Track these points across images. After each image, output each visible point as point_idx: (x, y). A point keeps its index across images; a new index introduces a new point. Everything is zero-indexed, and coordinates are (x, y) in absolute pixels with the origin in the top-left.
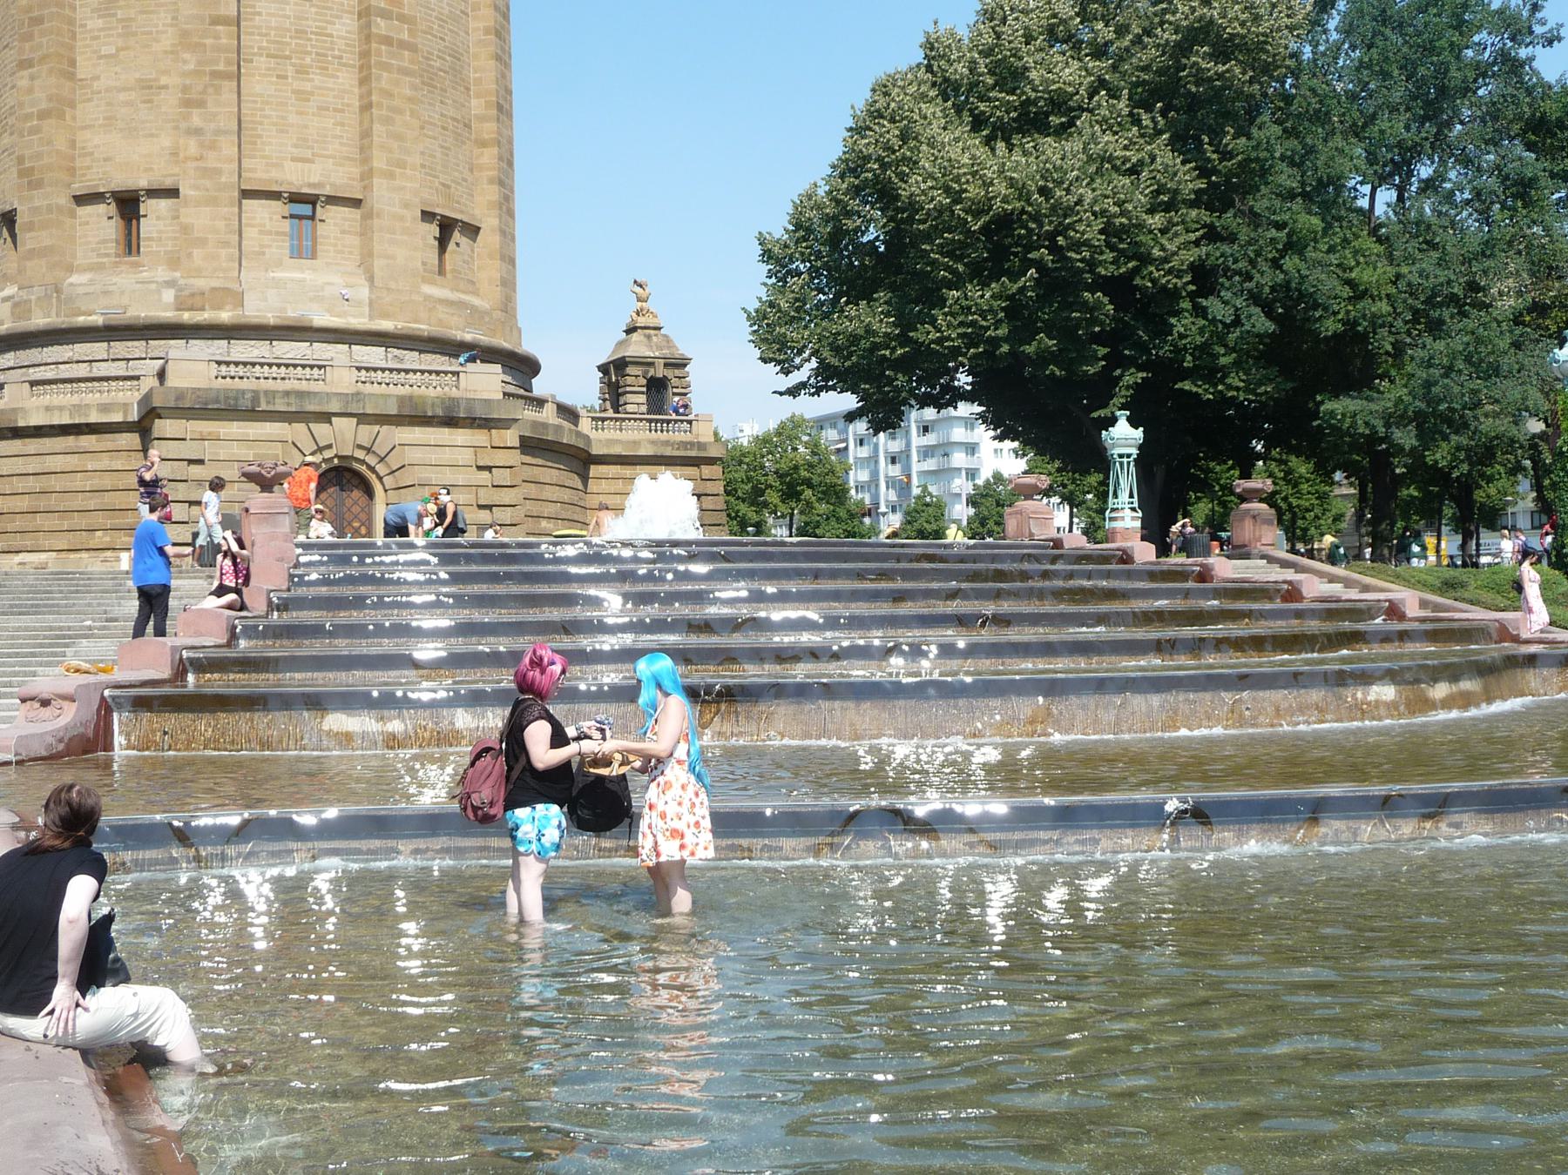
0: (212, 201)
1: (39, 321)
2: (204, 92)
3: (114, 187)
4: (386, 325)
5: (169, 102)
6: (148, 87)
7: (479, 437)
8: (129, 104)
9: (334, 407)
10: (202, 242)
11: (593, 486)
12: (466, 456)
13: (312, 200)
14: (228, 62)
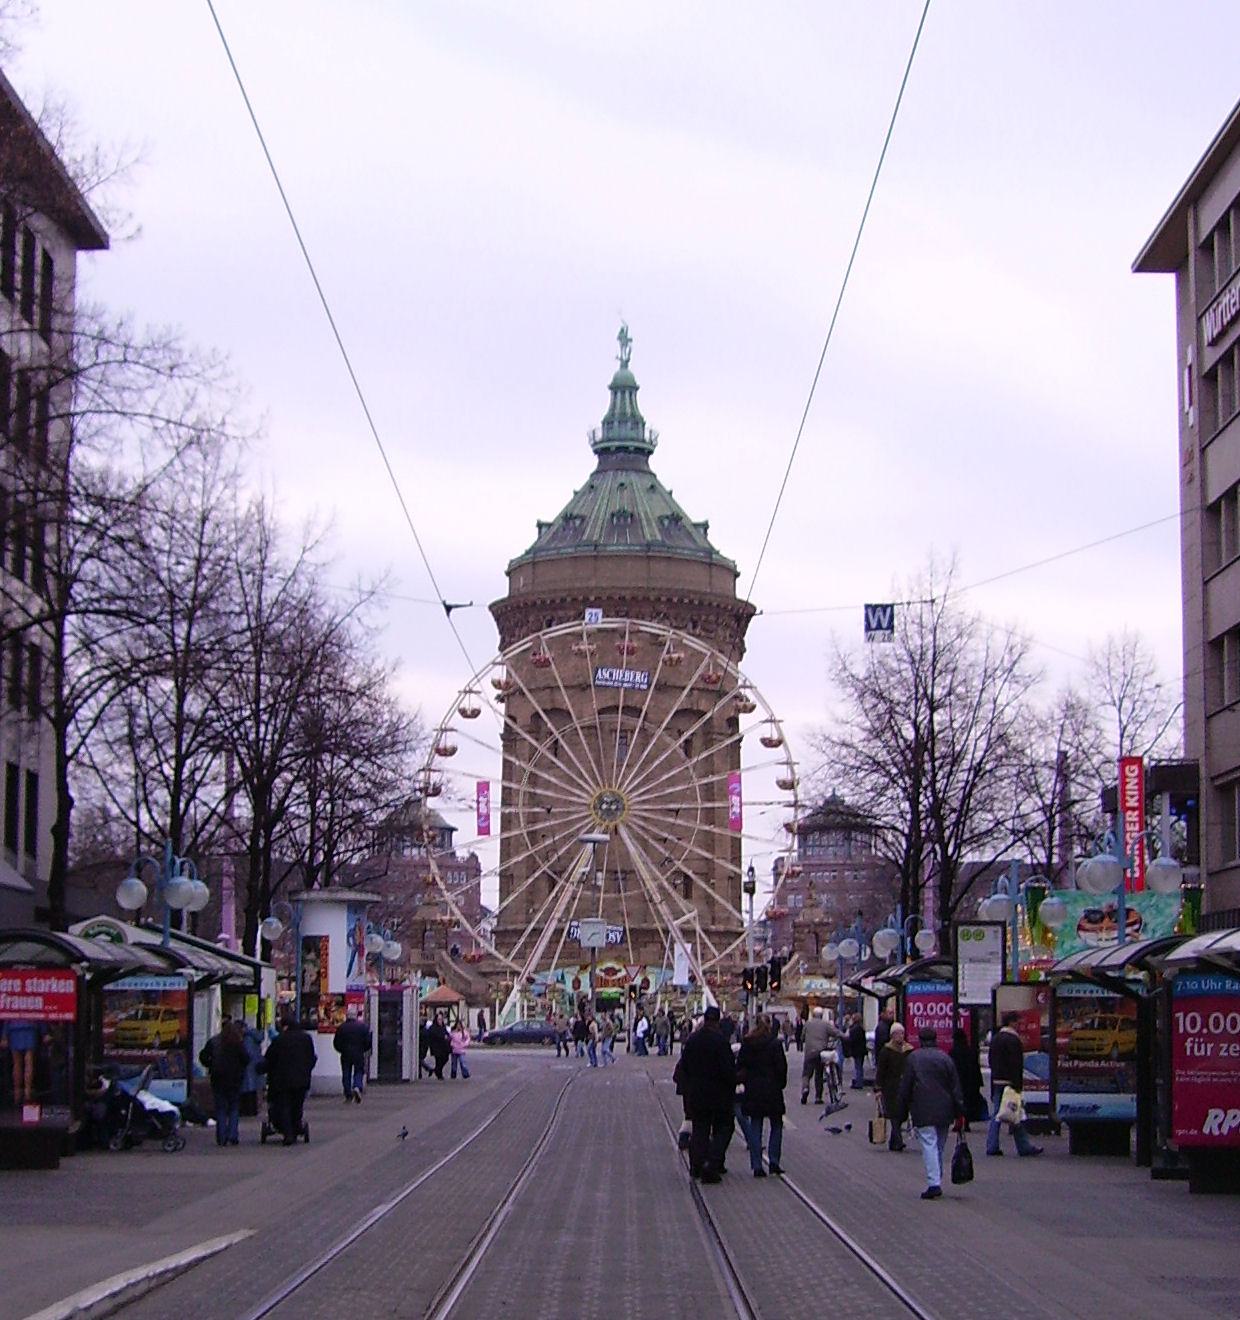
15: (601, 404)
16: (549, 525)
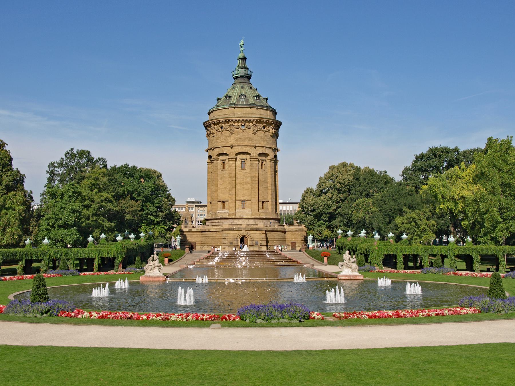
0: (232, 203)
1: (214, 217)
4: (253, 217)
5: (228, 190)
6: (226, 188)
7: (260, 232)
11: (286, 235)
12: (259, 235)
16: (221, 99)
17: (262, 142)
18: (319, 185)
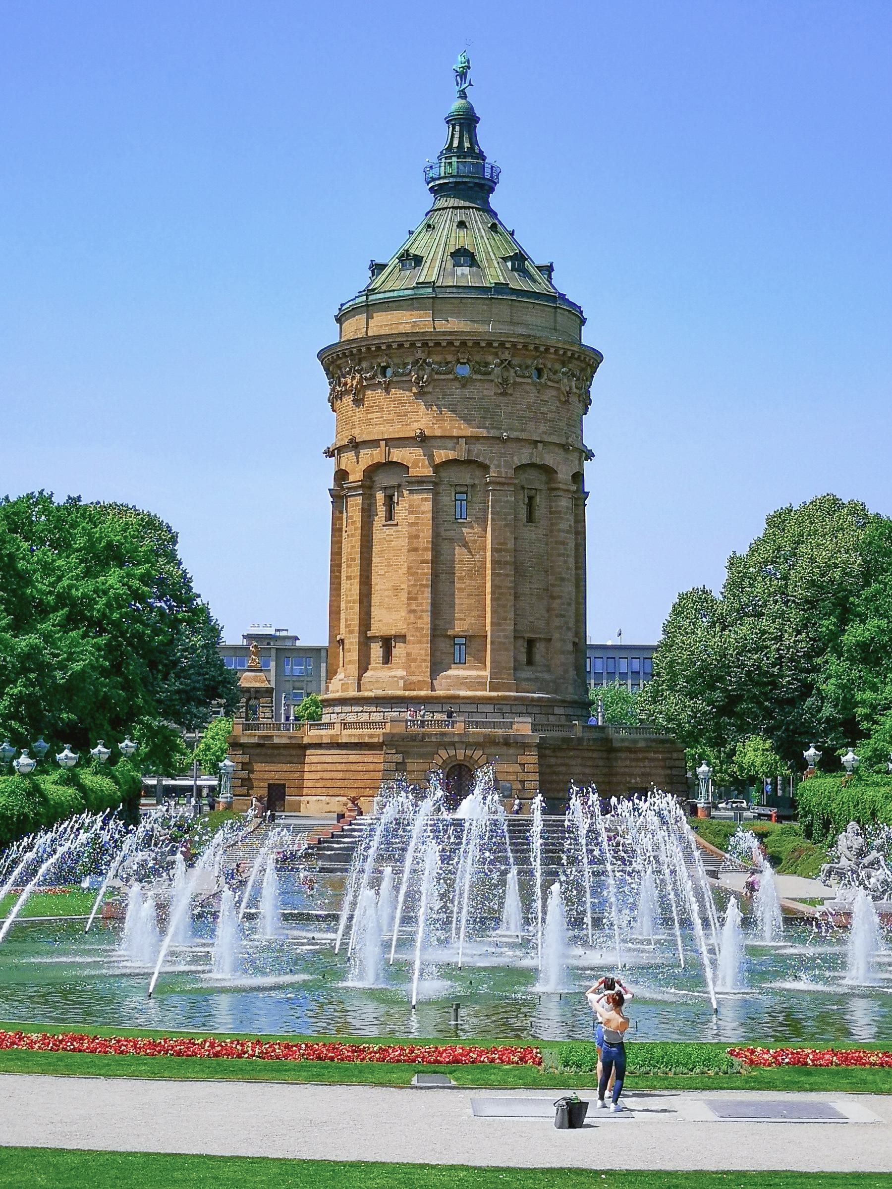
0: (420, 642)
1: (352, 693)
2: (417, 594)
3: (381, 634)
5: (404, 596)
6: (396, 589)
8: (387, 596)
9: (456, 739)
10: (415, 660)
13: (465, 637)
14: (427, 580)
15: (441, 136)
16: (382, 267)
17: (531, 425)
18: (735, 585)
